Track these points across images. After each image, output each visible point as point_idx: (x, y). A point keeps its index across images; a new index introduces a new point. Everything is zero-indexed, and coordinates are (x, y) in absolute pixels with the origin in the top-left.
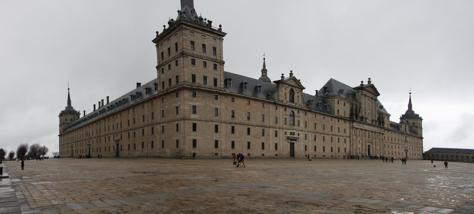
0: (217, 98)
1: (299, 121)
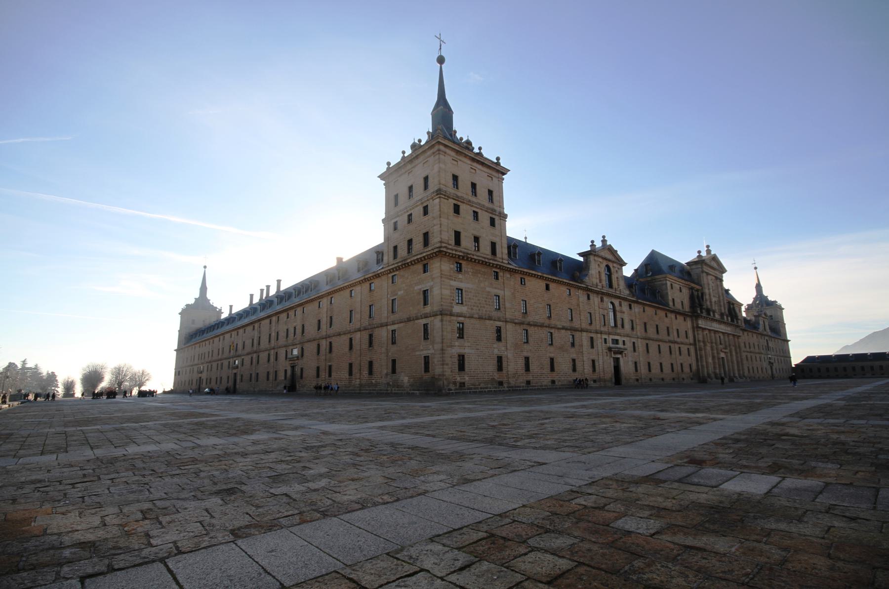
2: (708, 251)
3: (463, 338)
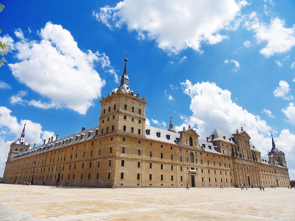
0: (140, 142)
2: (242, 130)
3: (123, 166)
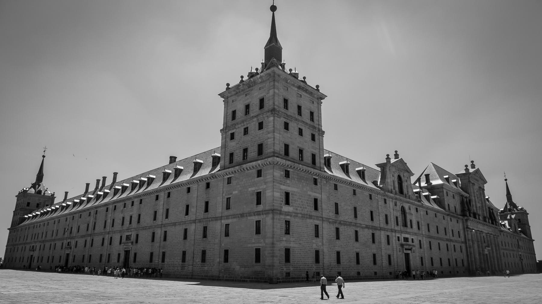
0: (315, 182)
1: (411, 221)
3: (289, 234)
